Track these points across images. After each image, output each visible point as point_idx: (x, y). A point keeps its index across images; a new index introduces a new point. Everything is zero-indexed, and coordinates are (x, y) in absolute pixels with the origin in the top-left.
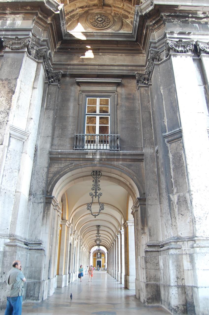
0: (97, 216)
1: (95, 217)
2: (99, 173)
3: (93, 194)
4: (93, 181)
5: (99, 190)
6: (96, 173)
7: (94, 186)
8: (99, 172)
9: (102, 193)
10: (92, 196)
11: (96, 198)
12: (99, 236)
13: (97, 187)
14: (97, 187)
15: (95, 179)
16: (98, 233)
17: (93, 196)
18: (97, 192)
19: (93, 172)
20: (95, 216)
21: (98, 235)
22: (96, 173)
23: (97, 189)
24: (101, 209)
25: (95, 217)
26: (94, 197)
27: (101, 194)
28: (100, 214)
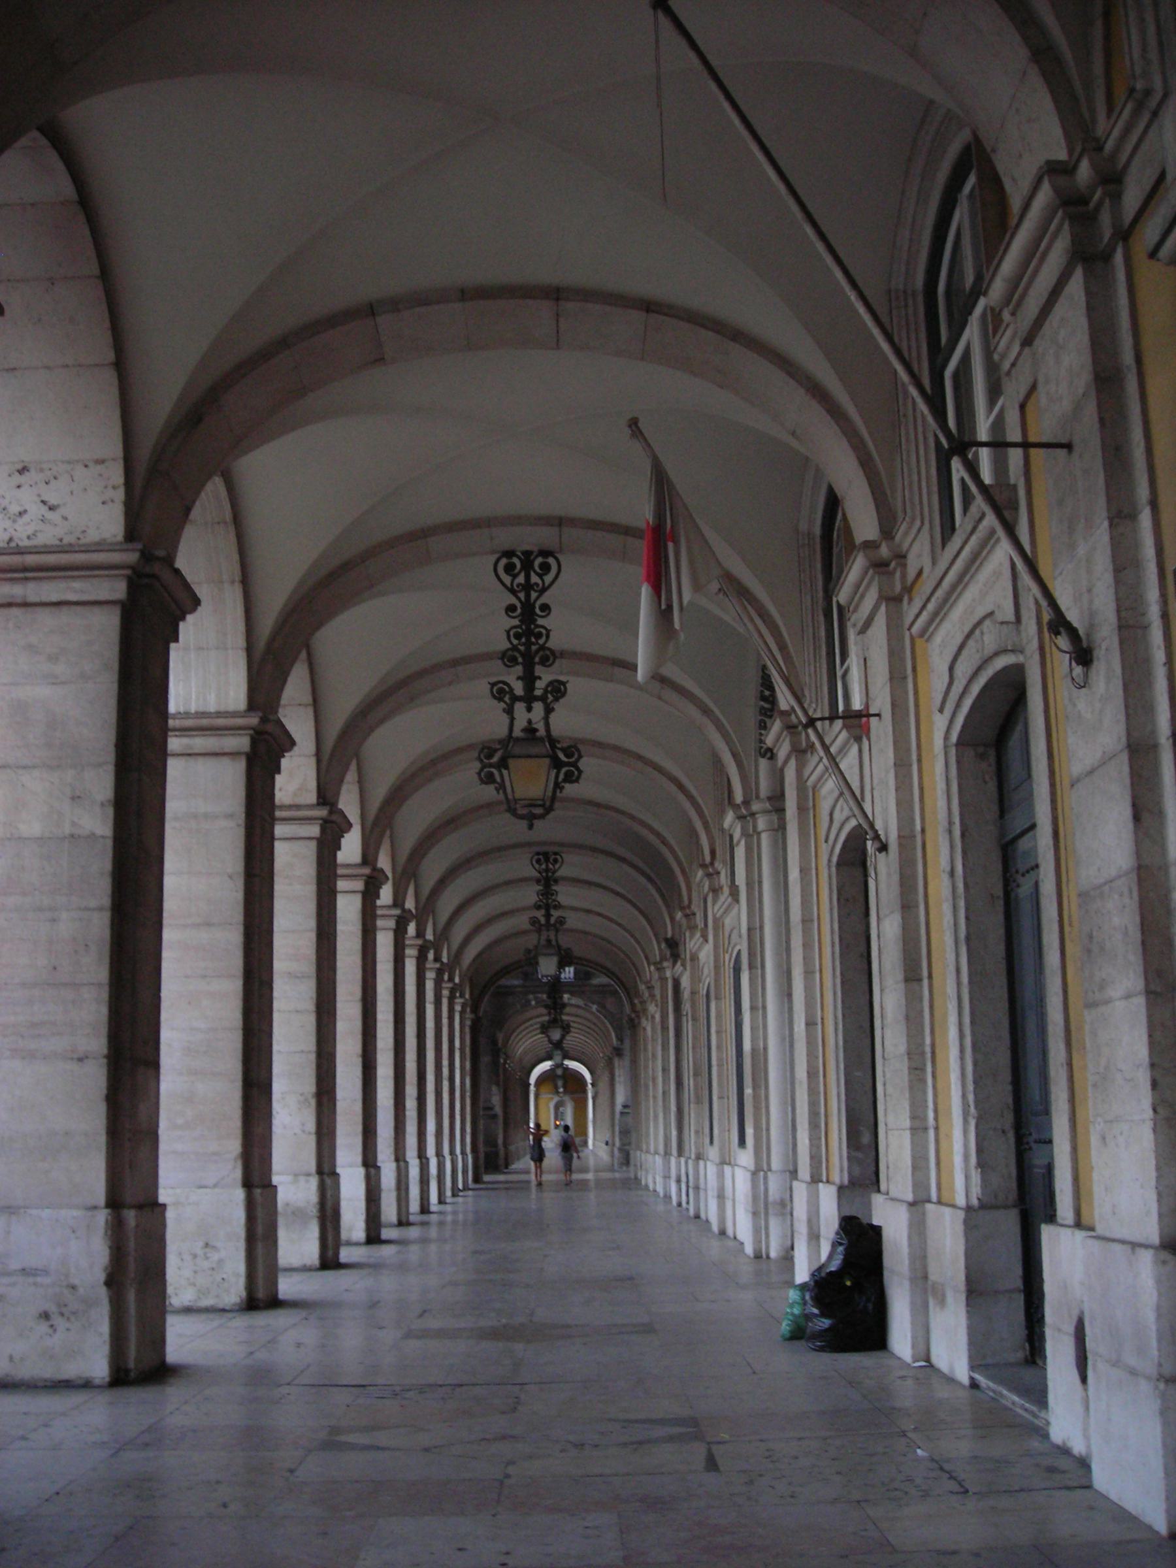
0: (542, 817)
1: (531, 827)
2: (540, 560)
3: (511, 690)
4: (511, 609)
5: (544, 662)
6: (527, 566)
7: (515, 642)
8: (545, 553)
9: (564, 684)
10: (507, 699)
11: (529, 709)
12: (552, 920)
13: (534, 648)
14: (534, 648)
15: (522, 595)
16: (547, 902)
17: (515, 699)
18: (537, 674)
19: (509, 554)
20: (531, 819)
21: (548, 916)
22: (527, 566)
23: (537, 659)
24: (561, 777)
25: (531, 827)
26: (520, 707)
27: (558, 690)
28: (557, 805)
